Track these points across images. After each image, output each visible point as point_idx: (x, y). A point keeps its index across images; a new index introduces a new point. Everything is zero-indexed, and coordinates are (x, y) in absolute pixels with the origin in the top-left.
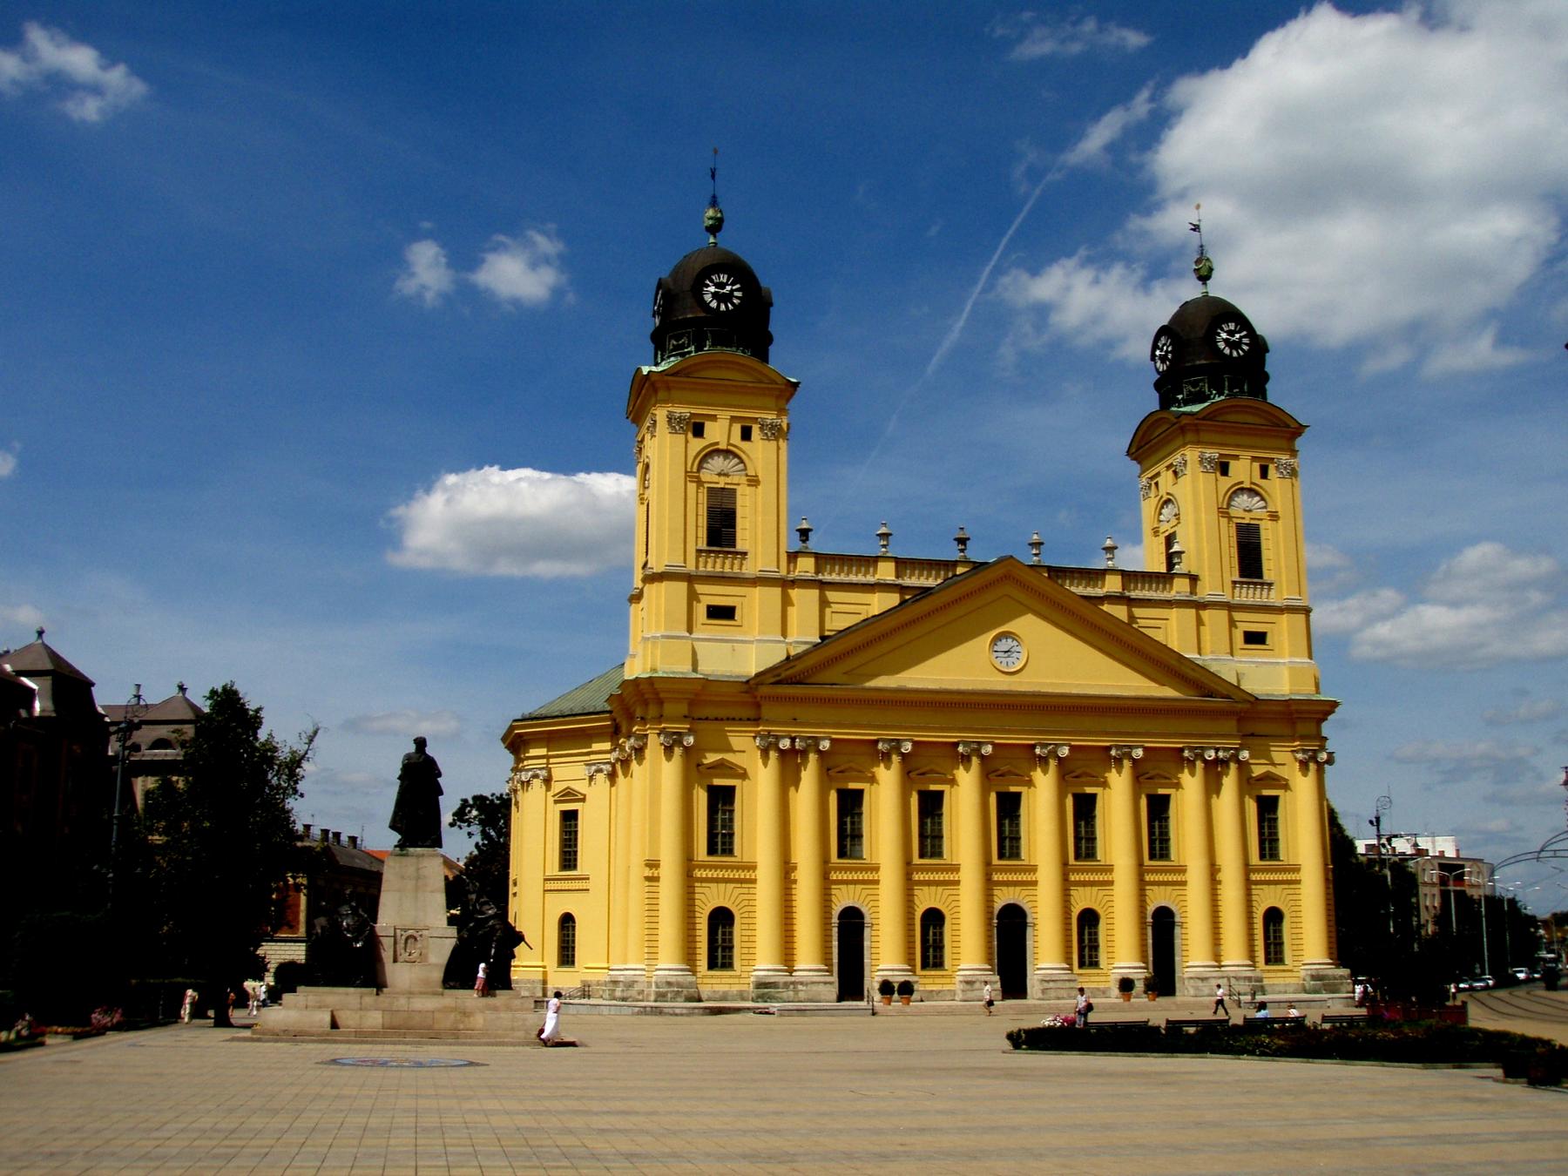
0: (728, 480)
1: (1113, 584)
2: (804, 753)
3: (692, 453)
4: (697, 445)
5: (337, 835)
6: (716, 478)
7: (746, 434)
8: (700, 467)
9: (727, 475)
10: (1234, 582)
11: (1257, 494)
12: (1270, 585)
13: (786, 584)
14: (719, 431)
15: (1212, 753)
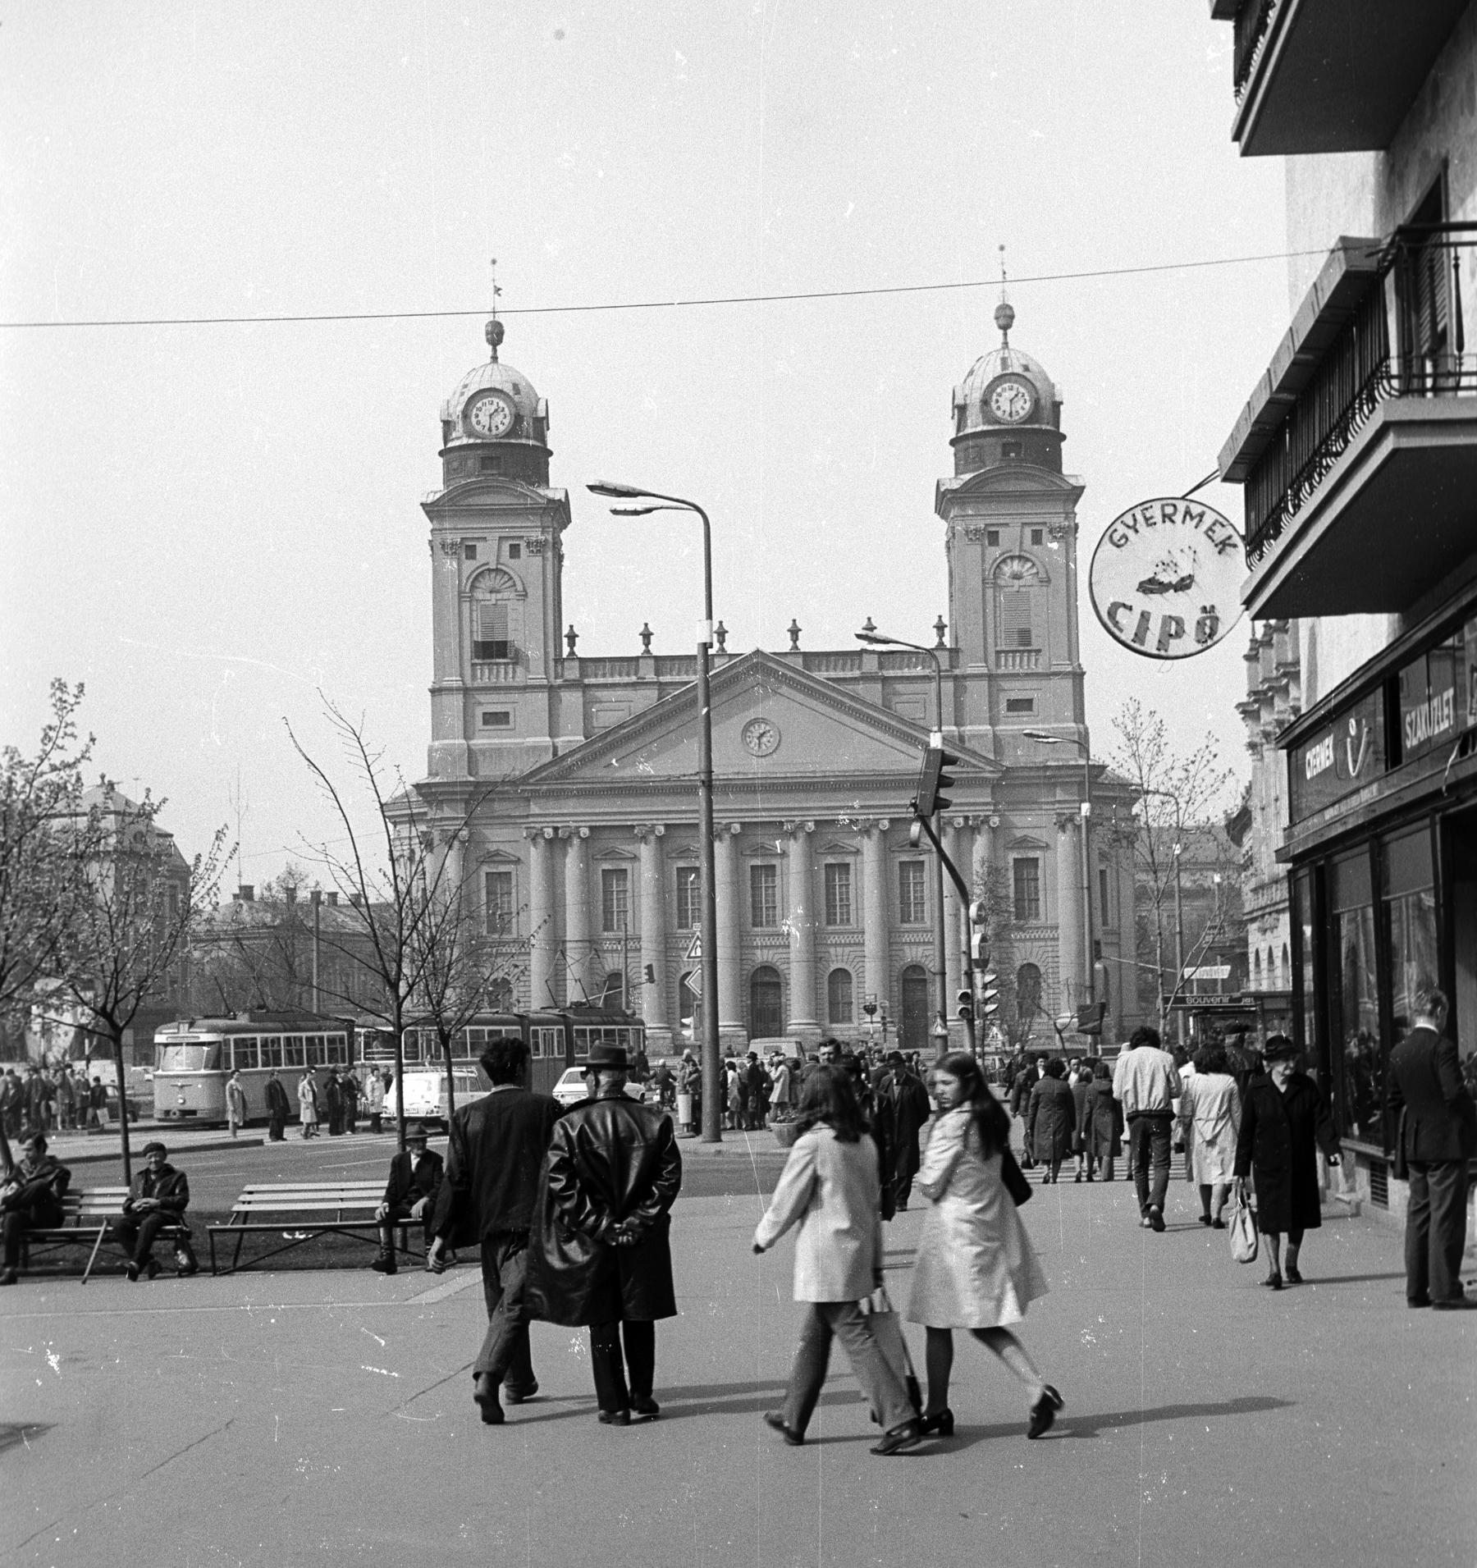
0: (499, 596)
1: (870, 665)
2: (566, 841)
3: (465, 575)
4: (469, 566)
5: (333, 895)
6: (488, 596)
7: (515, 551)
8: (473, 587)
9: (498, 592)
10: (998, 653)
11: (1028, 560)
12: (1038, 651)
13: (552, 689)
14: (486, 553)
15: (961, 820)
